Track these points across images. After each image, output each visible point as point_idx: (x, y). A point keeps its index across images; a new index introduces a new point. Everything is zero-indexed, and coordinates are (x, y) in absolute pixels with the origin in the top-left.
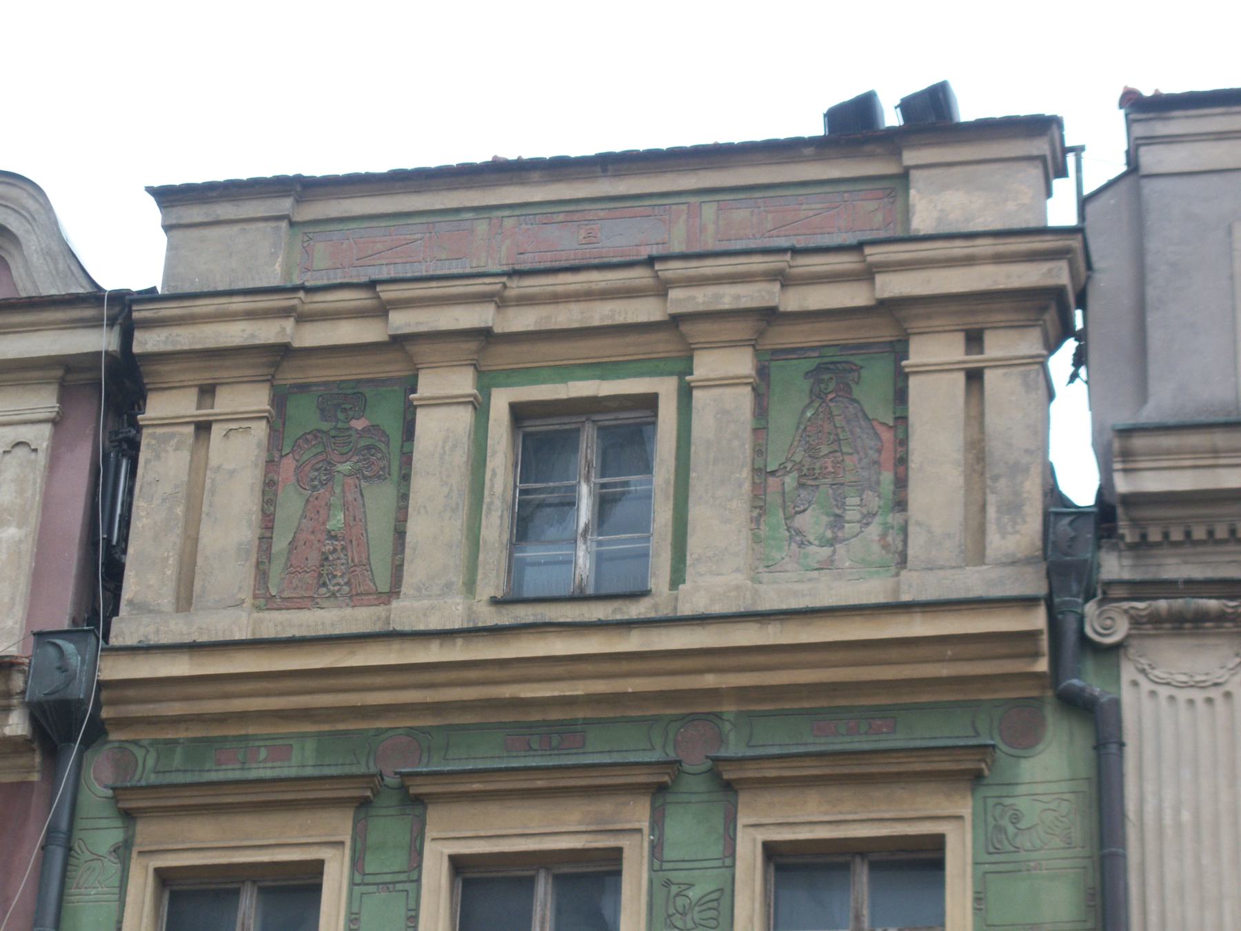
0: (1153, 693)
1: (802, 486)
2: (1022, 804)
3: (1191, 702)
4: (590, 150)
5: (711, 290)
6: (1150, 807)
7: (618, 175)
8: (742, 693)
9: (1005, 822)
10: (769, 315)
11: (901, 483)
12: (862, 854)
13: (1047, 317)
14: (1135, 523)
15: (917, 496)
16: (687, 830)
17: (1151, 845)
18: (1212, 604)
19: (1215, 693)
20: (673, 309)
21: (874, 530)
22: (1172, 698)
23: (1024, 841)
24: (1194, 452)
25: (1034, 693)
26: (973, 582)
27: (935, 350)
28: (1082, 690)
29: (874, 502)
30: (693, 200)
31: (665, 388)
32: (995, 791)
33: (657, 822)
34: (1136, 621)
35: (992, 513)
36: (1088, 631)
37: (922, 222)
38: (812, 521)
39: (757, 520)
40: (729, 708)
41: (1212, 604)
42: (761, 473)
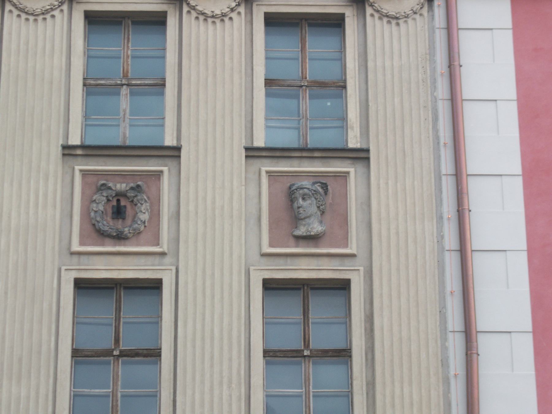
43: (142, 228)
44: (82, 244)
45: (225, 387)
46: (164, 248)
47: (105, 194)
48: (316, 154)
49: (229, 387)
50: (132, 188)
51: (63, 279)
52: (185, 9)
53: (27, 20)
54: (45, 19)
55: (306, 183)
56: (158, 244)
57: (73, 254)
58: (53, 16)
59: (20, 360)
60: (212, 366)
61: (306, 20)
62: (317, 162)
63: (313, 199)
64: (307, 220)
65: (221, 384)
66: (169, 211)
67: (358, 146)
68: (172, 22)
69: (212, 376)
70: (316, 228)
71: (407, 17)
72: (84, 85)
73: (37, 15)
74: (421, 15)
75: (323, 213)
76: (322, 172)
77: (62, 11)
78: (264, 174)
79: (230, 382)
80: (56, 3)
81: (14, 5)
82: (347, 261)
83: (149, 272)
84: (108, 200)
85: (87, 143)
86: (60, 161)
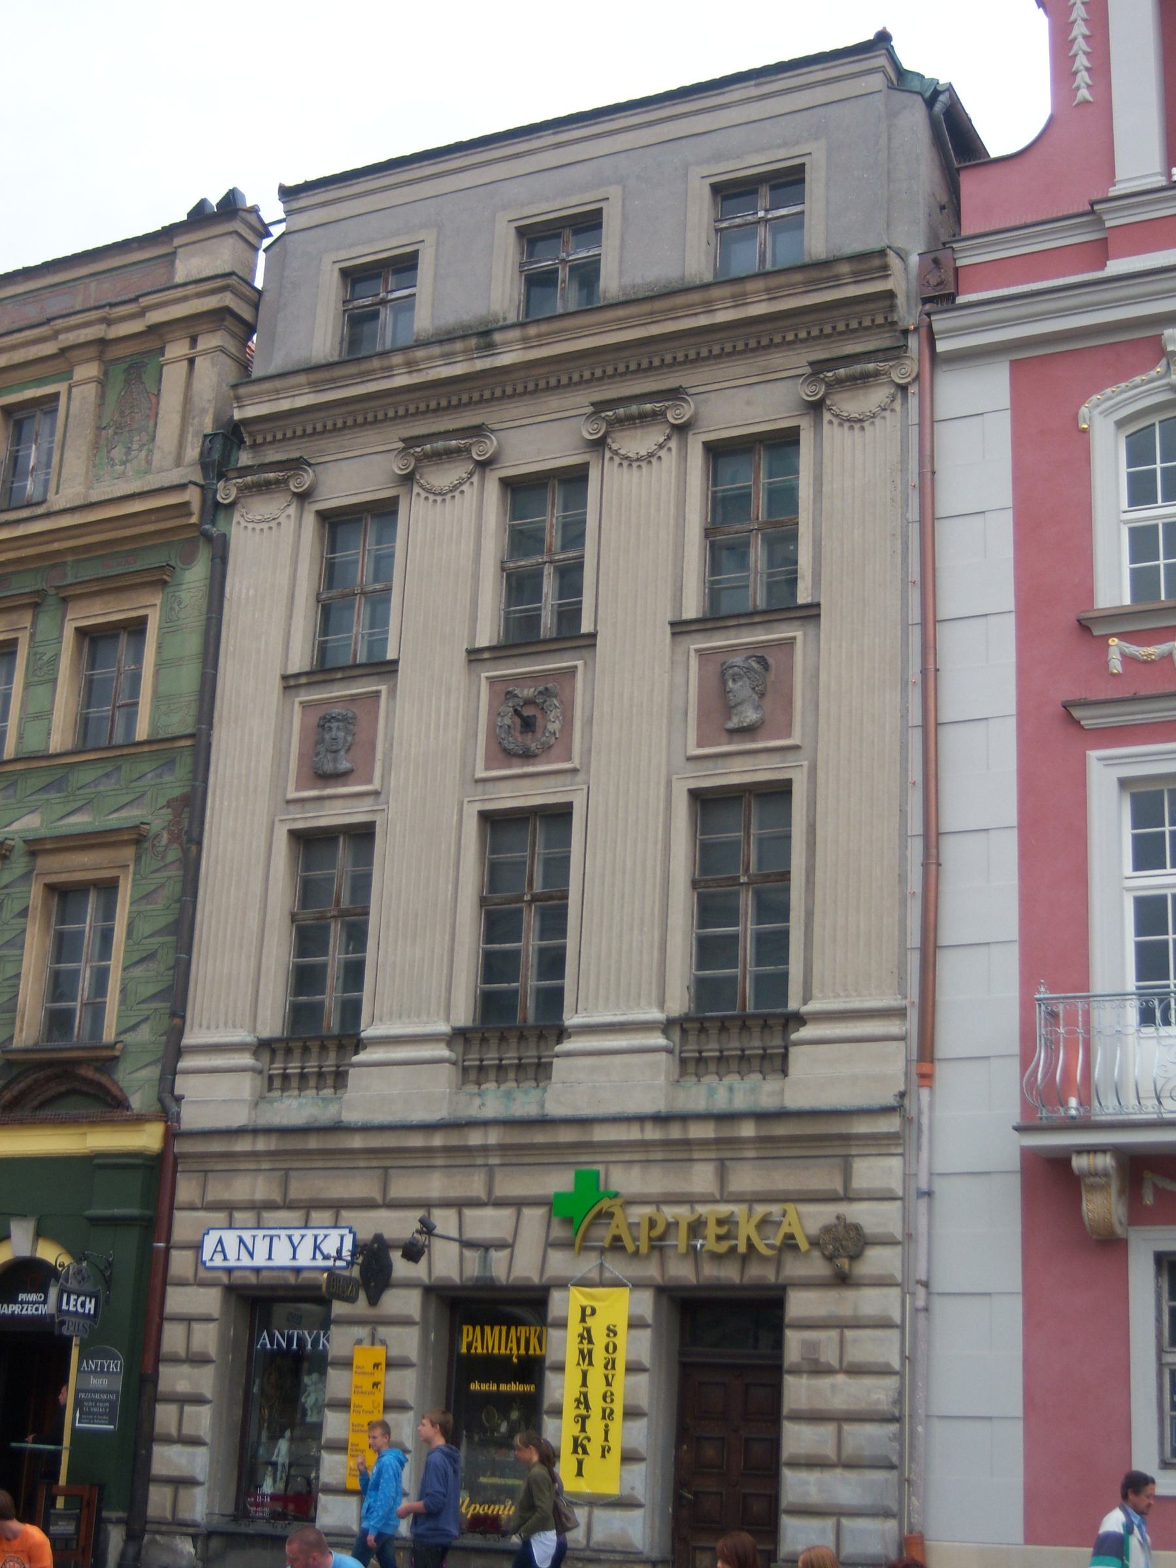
1: (116, 433)
4: (38, 261)
5: (75, 333)
7: (55, 272)
8: (73, 550)
10: (102, 343)
11: (155, 427)
12: (125, 628)
13: (226, 323)
14: (250, 434)
15: (160, 433)
16: (46, 623)
18: (272, 476)
19: (273, 524)
20: (61, 346)
21: (144, 453)
22: (254, 529)
23: (182, 615)
24: (268, 392)
26: (174, 477)
27: (177, 349)
29: (145, 437)
30: (87, 281)
31: (61, 387)
33: (34, 623)
34: (240, 489)
35: (190, 436)
36: (218, 498)
37: (179, 278)
38: (118, 453)
39: (95, 455)
40: (70, 559)
41: (272, 476)
42: (99, 429)
43: (553, 741)
44: (488, 768)
45: (636, 932)
46: (576, 763)
48: (757, 619)
50: (540, 693)
52: (608, 455)
53: (435, 501)
54: (453, 497)
55: (738, 660)
56: (570, 759)
58: (462, 492)
61: (761, 442)
62: (759, 629)
63: (745, 679)
64: (739, 708)
66: (583, 713)
67: (809, 600)
68: (594, 475)
70: (750, 716)
71: (874, 416)
72: (503, 570)
73: (445, 494)
74: (893, 410)
75: (762, 695)
76: (762, 642)
77: (472, 483)
78: (692, 653)
80: (465, 475)
81: (422, 486)
82: (790, 756)
83: (558, 795)
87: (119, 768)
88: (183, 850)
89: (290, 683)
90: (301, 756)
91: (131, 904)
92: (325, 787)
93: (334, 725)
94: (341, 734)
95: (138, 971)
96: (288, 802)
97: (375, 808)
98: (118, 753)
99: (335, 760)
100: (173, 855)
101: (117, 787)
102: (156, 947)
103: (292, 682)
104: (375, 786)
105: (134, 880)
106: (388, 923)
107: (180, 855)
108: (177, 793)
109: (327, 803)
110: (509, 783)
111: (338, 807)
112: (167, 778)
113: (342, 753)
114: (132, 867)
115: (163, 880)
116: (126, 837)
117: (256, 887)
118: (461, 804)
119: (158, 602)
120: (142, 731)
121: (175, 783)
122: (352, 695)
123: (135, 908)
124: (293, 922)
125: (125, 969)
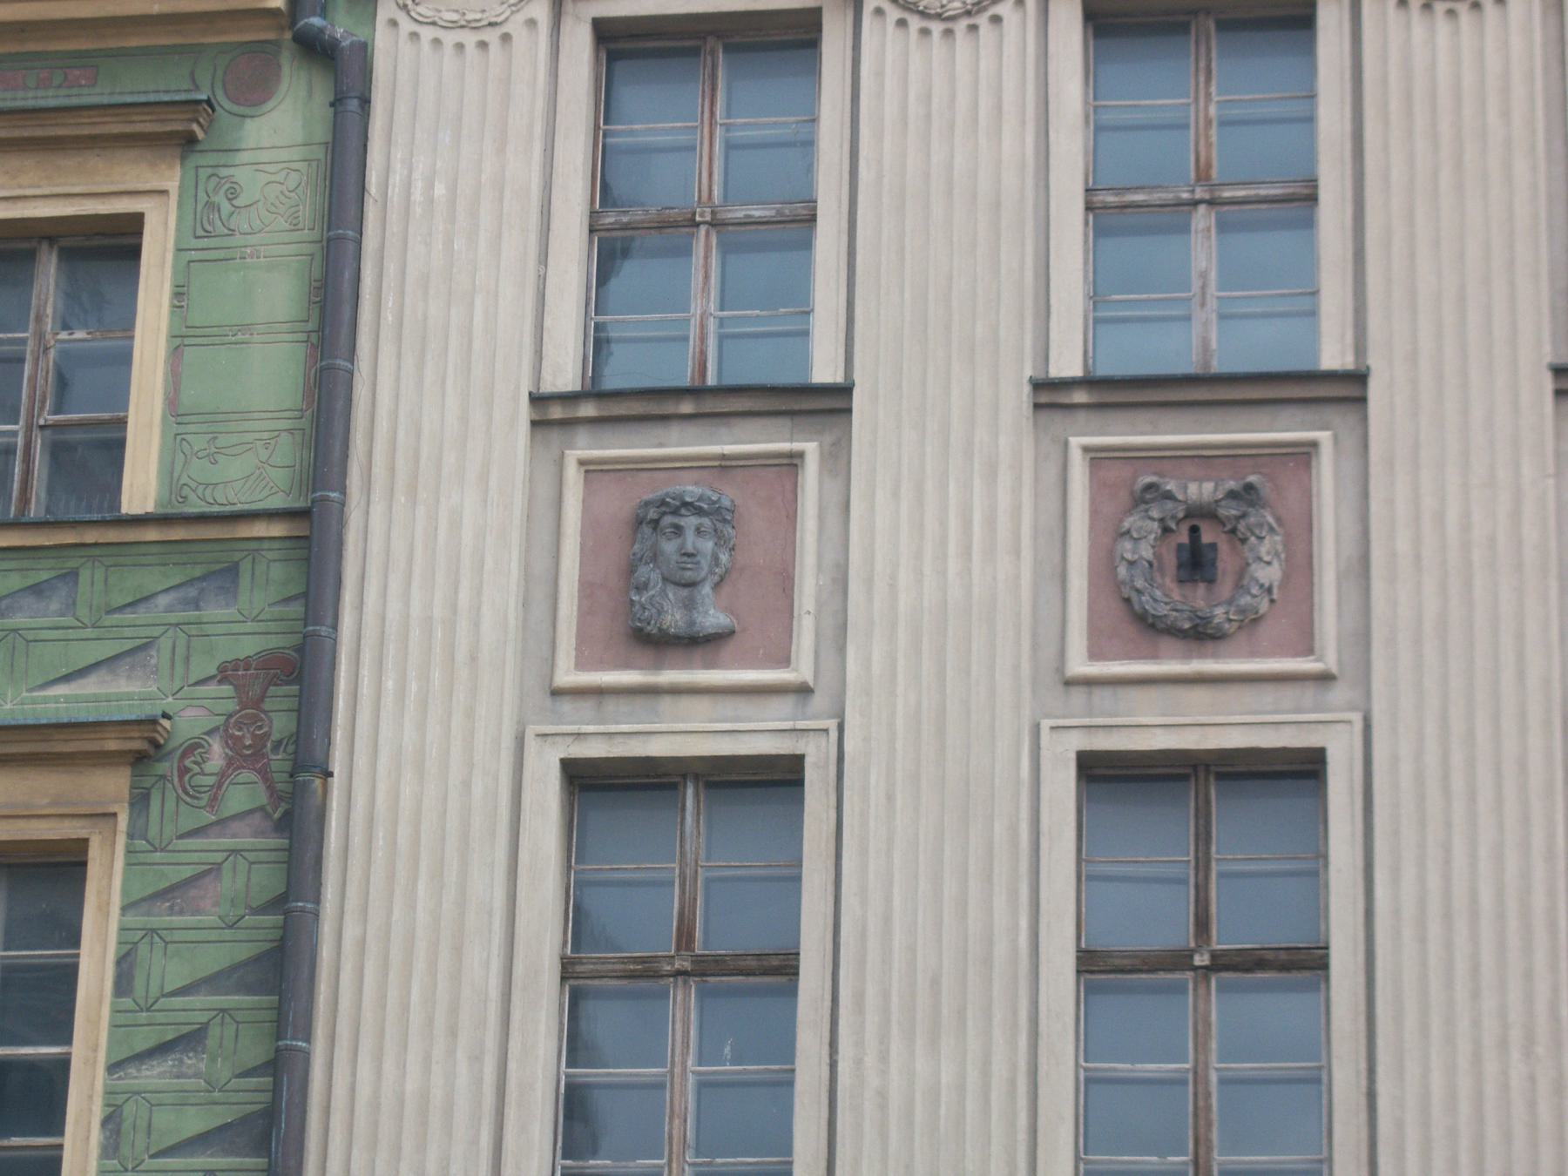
0: (414, 36)
2: (241, 175)
3: (460, 46)
6: (396, 179)
9: (220, 199)
12: (51, 239)
17: (394, 226)
19: (491, 36)
22: (437, 42)
23: (241, 222)
25: (271, 36)
28: (322, 30)
32: (210, 159)
43: (1264, 606)
44: (1095, 654)
45: (1515, 1055)
46: (1328, 658)
47: (1155, 514)
49: (1528, 1053)
50: (1232, 495)
51: (1044, 753)
53: (925, 32)
54: (973, 28)
56: (1308, 650)
57: (1069, 683)
58: (996, 20)
59: (935, 982)
60: (1476, 995)
65: (1503, 1044)
66: (1338, 555)
69: (1476, 1023)
72: (1089, 207)
79: (1530, 1039)
83: (1288, 730)
84: (1166, 530)
85: (1102, 371)
86: (1027, 423)
87: (73, 575)
88: (271, 788)
89: (550, 414)
90: (587, 588)
91: (124, 909)
92: (658, 666)
93: (689, 522)
94: (708, 545)
95: (152, 1075)
96: (557, 693)
97: (801, 724)
98: (69, 537)
99: (689, 605)
100: (243, 794)
101: (64, 621)
102: (203, 1018)
103: (556, 412)
104: (801, 670)
105: (129, 851)
106: (860, 997)
107: (263, 798)
108: (248, 647)
109: (666, 703)
110: (1153, 693)
111: (698, 714)
112: (215, 612)
113: (706, 589)
114: (123, 822)
115: (219, 857)
116: (112, 745)
117: (488, 888)
118: (1036, 730)
119: (173, 185)
120: (140, 488)
121: (244, 624)
122: (724, 457)
123: (133, 920)
124: (563, 979)
125: (113, 1068)
